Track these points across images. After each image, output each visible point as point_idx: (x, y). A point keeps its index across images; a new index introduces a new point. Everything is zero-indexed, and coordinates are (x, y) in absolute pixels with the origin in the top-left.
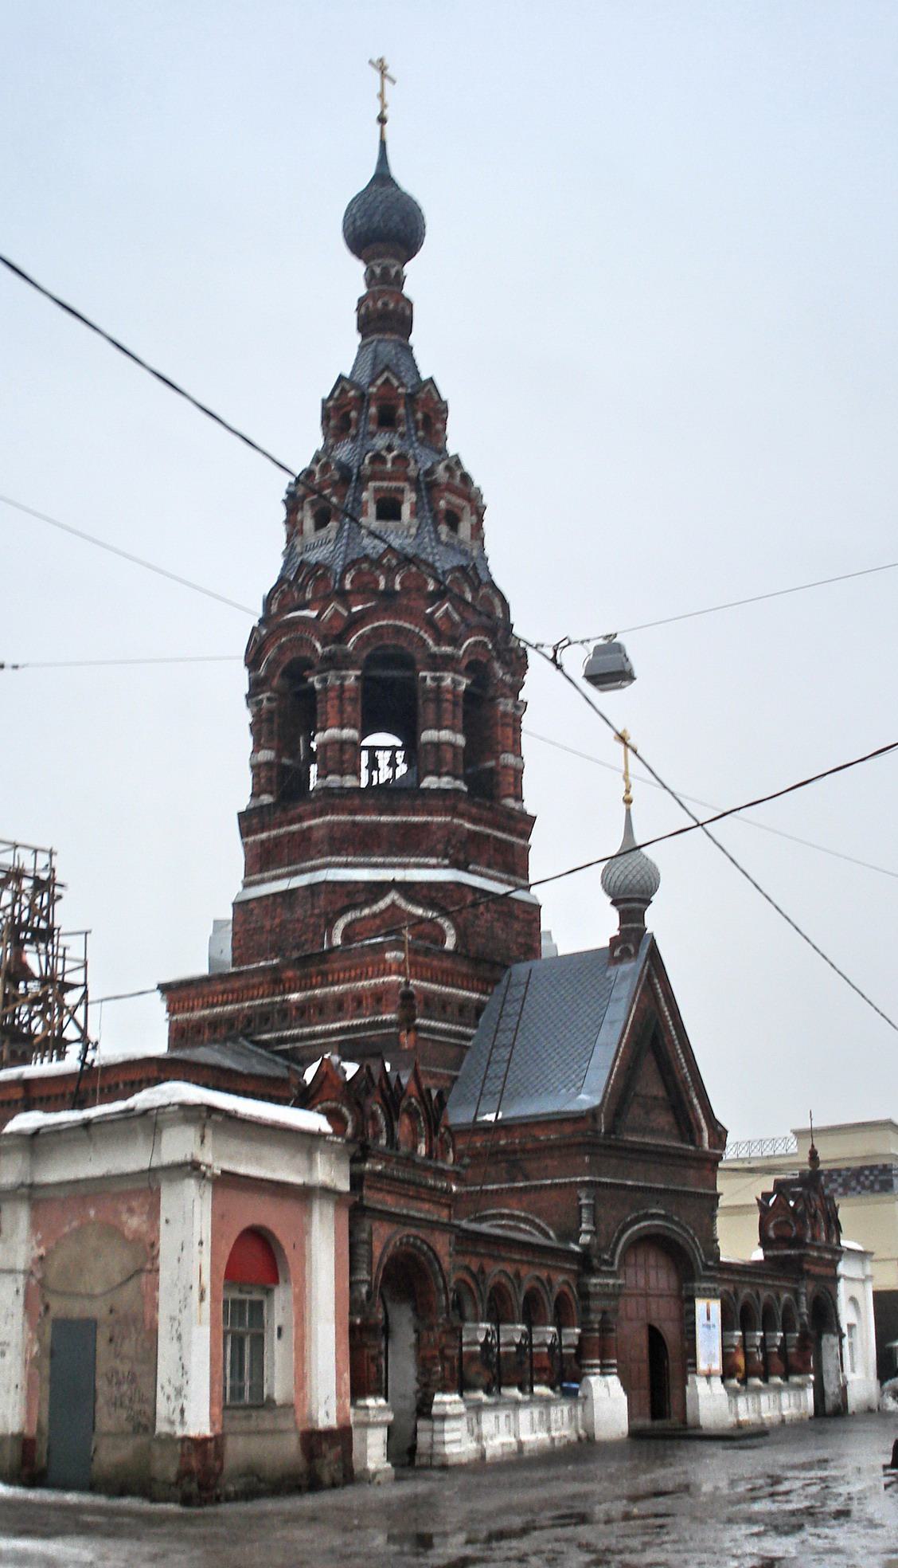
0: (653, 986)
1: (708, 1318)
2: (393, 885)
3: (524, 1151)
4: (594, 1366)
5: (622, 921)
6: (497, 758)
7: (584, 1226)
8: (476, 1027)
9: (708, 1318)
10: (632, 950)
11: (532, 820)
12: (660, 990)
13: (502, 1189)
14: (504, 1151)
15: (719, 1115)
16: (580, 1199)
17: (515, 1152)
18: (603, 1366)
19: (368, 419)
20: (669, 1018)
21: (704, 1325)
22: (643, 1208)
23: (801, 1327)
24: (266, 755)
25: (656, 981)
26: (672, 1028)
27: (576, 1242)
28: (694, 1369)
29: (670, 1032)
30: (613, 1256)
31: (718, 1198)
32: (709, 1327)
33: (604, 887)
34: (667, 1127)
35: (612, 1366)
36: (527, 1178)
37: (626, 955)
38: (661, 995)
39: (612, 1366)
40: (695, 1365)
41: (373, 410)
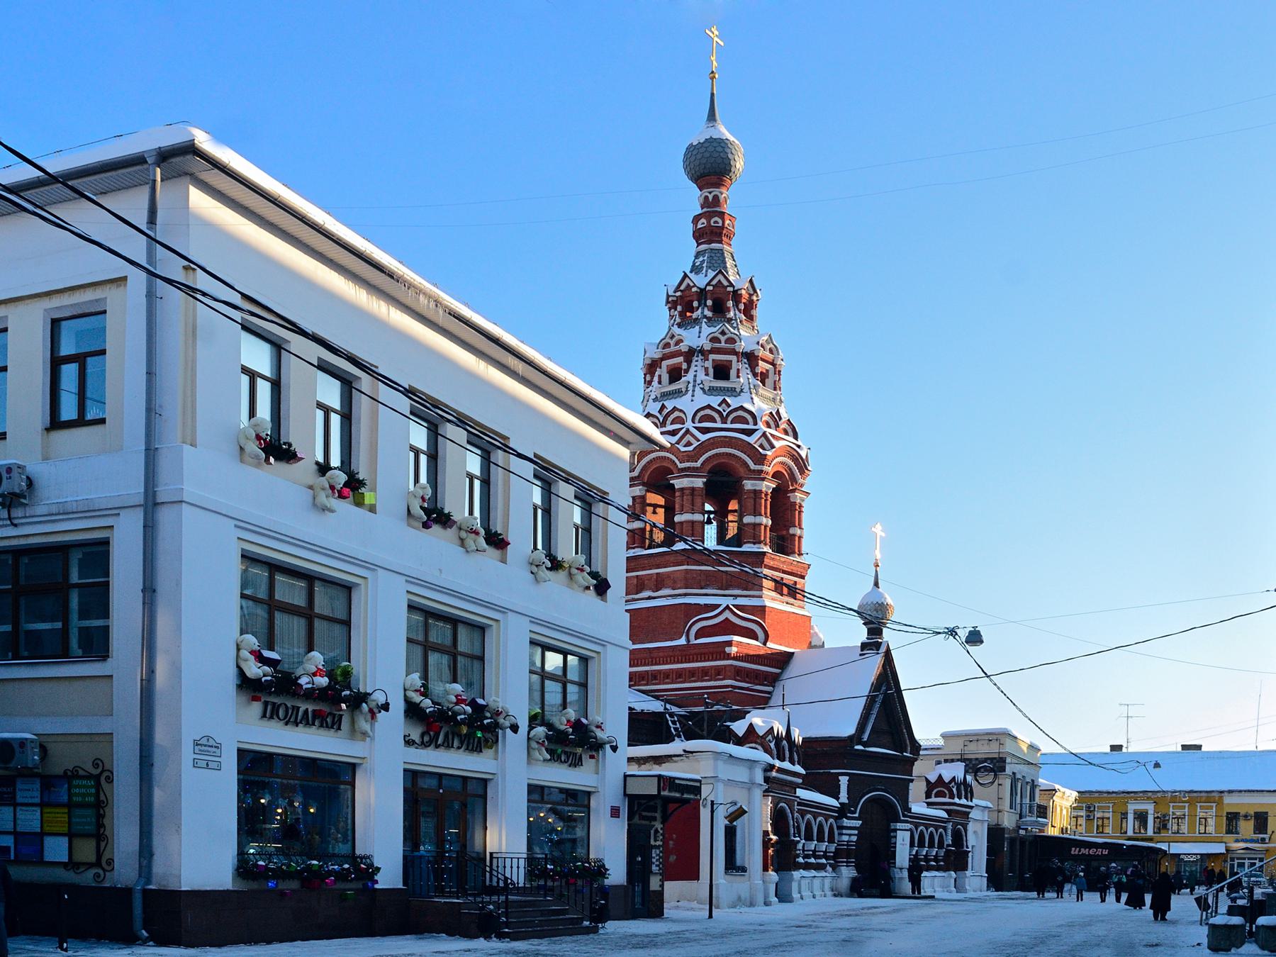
41: (709, 303)
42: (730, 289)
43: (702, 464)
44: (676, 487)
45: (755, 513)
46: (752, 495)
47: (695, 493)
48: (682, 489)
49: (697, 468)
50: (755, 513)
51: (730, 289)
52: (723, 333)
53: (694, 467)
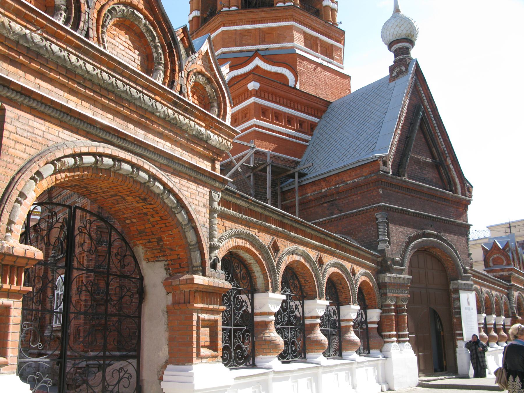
0: (418, 92)
1: (469, 303)
2: (256, 53)
3: (338, 193)
4: (390, 336)
5: (396, 56)
7: (381, 237)
8: (311, 135)
9: (469, 303)
10: (404, 69)
11: (344, 32)
12: (423, 95)
13: (325, 220)
14: (325, 196)
15: (467, 175)
16: (377, 219)
17: (332, 195)
18: (398, 336)
20: (431, 113)
21: (466, 308)
22: (423, 229)
23: (512, 314)
24: (196, 13)
25: (421, 89)
26: (433, 119)
27: (375, 249)
28: (461, 337)
29: (432, 121)
30: (403, 259)
31: (469, 228)
32: (469, 309)
33: (382, 38)
34: (434, 180)
35: (404, 336)
36: (341, 211)
37: (400, 73)
38: (425, 98)
39: (404, 336)
40: (462, 335)
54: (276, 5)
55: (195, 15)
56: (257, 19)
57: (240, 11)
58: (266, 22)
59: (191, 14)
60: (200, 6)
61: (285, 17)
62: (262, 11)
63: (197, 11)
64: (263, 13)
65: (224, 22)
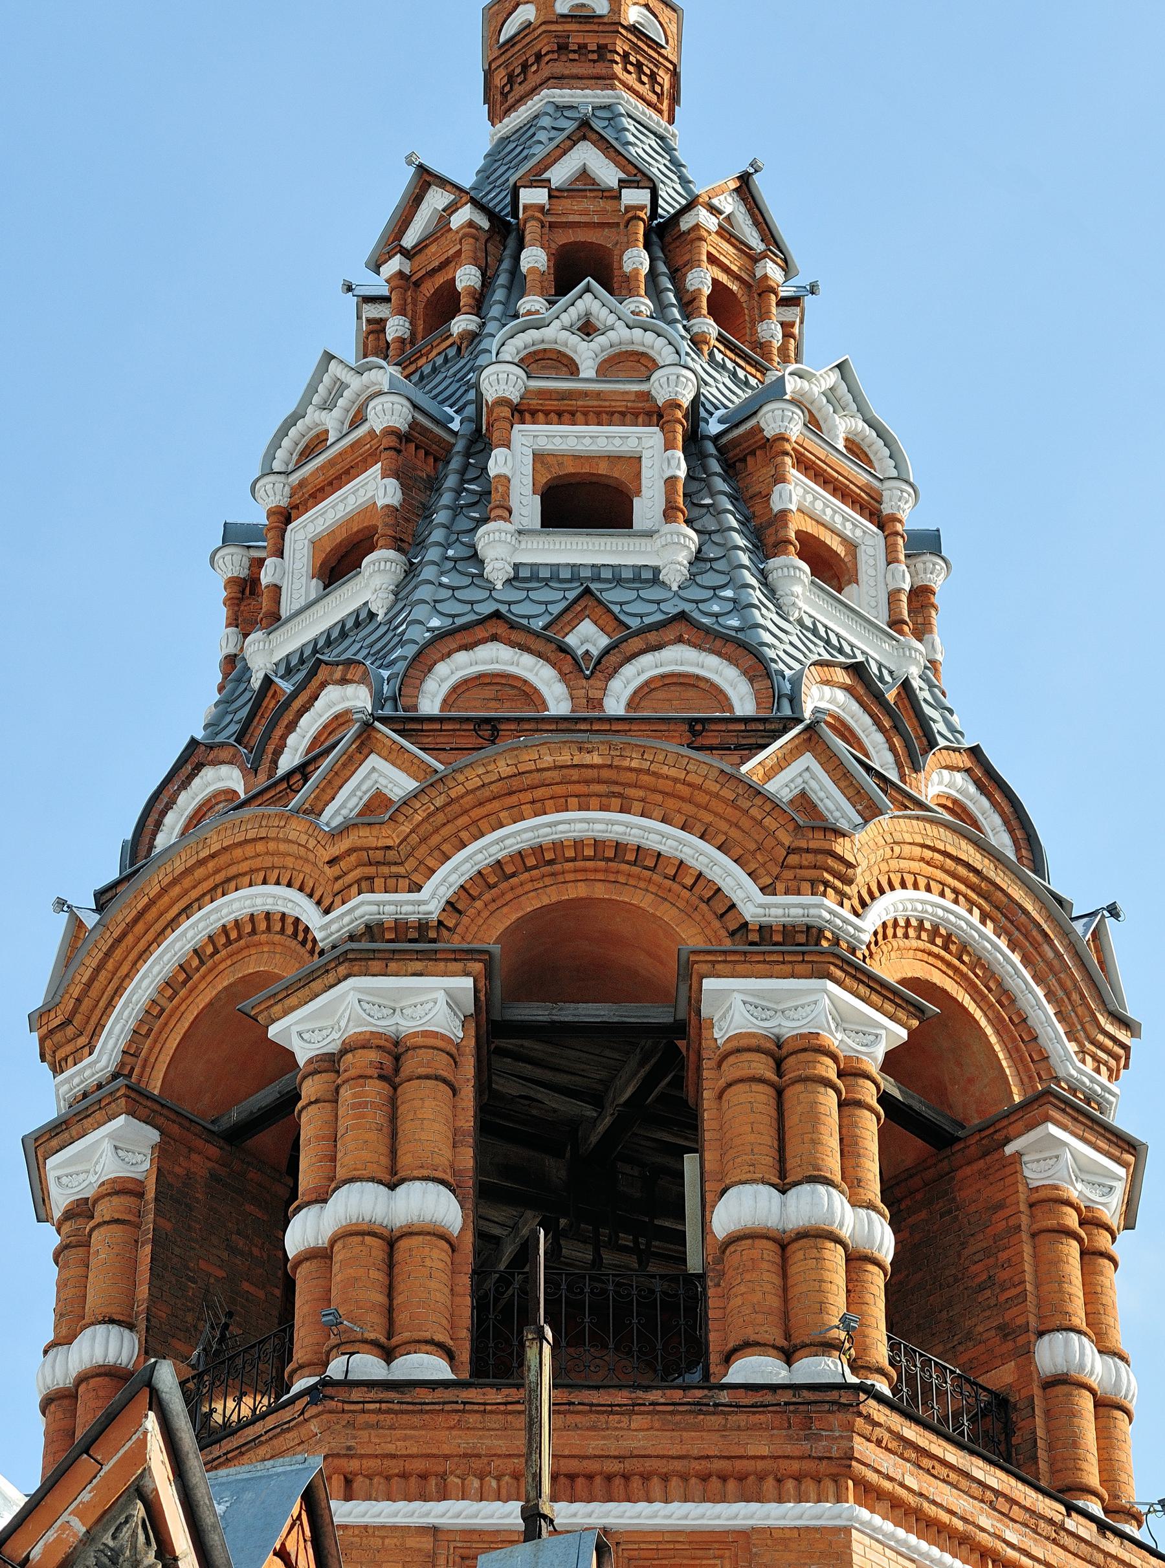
6: (1026, 1354)
19: (517, 284)
42: (636, 197)
43: (451, 905)
44: (301, 1059)
45: (782, 1174)
46: (762, 1066)
47: (410, 1065)
48: (329, 1063)
49: (422, 926)
50: (782, 1174)
51: (636, 197)
52: (587, 329)
53: (400, 927)
54: (728, 1359)
55: (99, 1359)
56: (593, 1466)
57: (472, 1394)
58: (656, 1484)
59: (63, 1340)
60: (143, 1291)
61: (796, 1466)
62: (631, 1409)
63: (115, 1330)
64: (638, 1421)
65: (354, 1465)
